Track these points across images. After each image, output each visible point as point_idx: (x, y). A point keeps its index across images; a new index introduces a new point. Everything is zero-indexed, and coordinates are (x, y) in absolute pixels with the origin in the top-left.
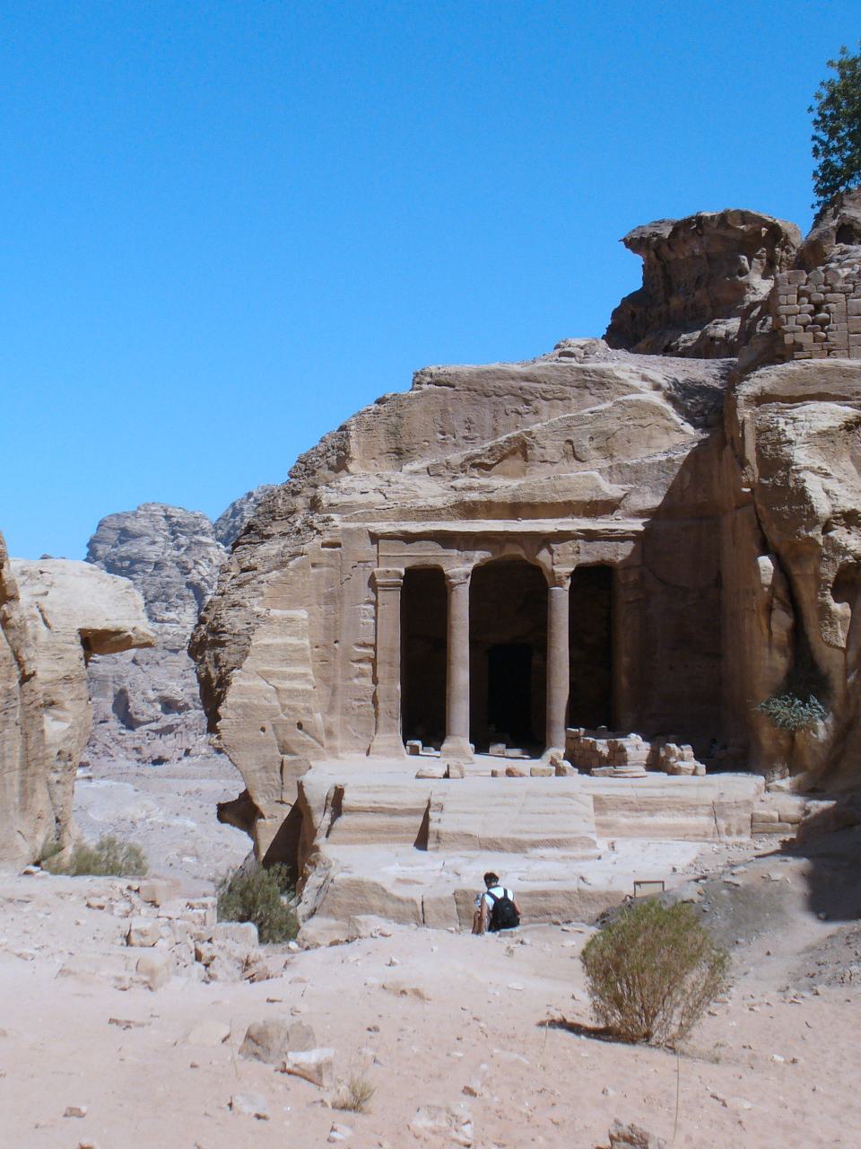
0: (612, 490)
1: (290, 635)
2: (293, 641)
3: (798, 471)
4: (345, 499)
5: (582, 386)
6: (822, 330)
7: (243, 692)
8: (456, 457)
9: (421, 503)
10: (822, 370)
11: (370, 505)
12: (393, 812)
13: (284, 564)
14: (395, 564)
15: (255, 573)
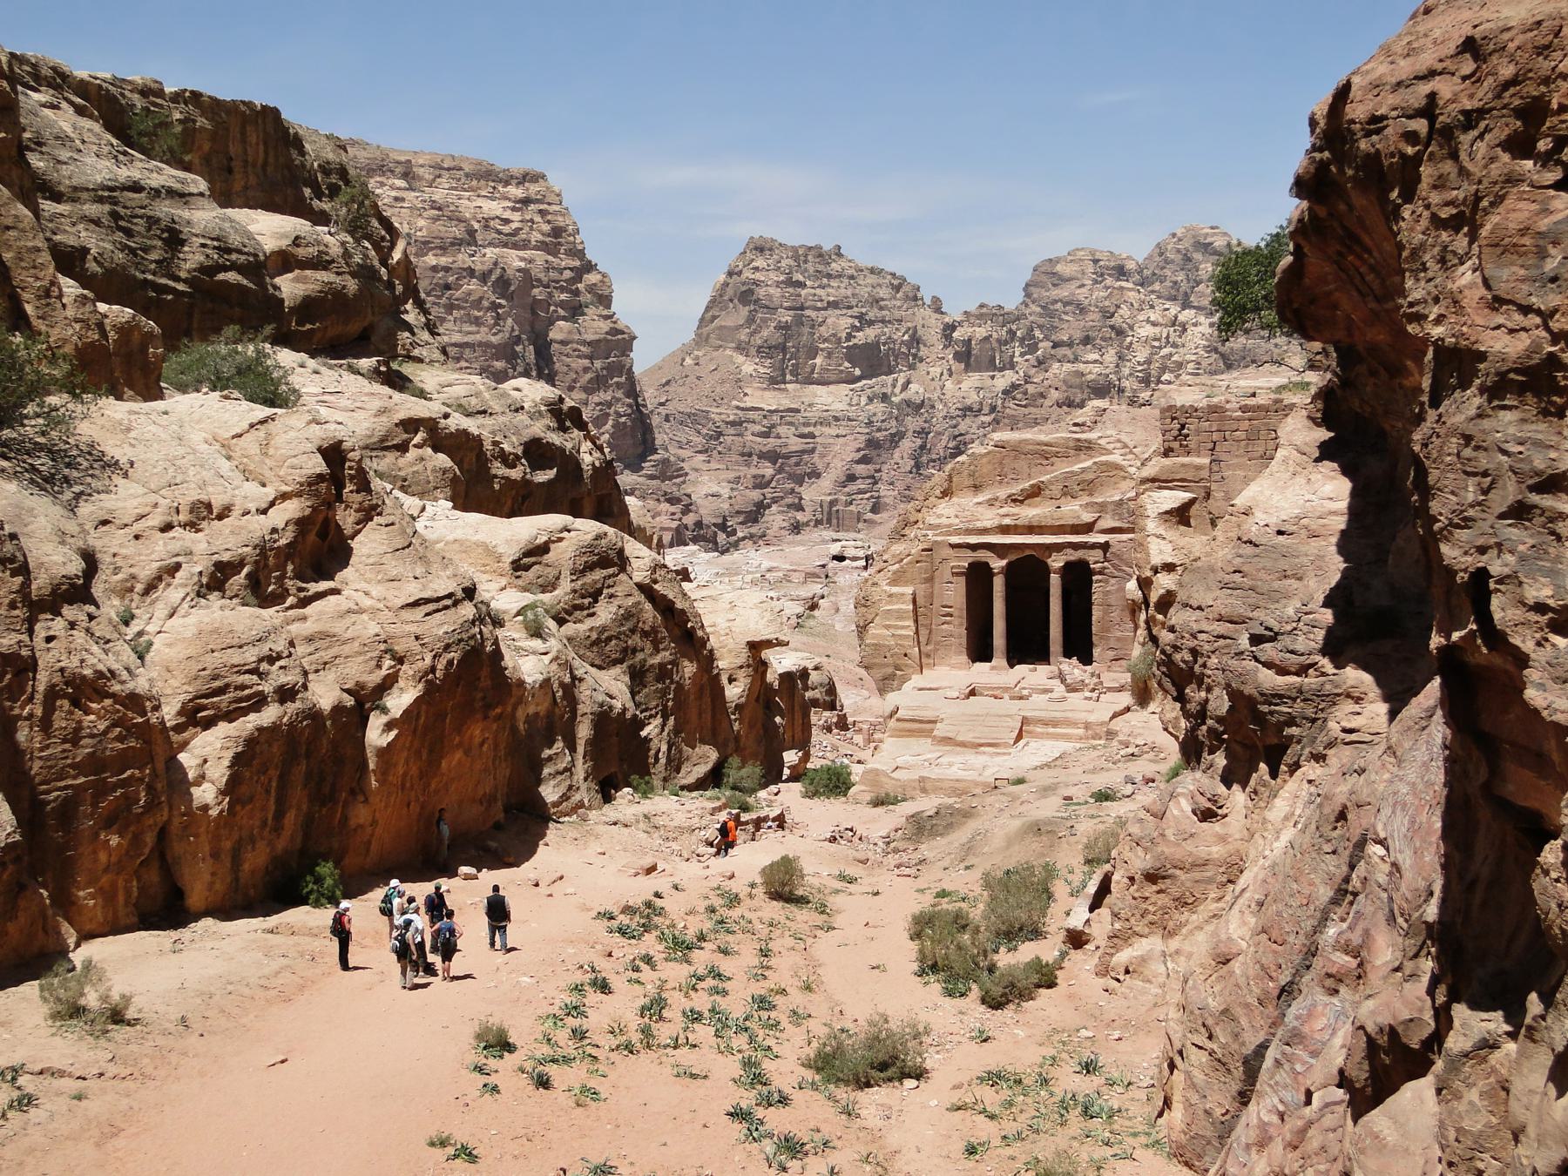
0: (1087, 517)
2: (903, 607)
4: (938, 521)
5: (1078, 449)
7: (875, 636)
8: (1002, 493)
10: (1183, 465)
11: (950, 526)
12: (921, 722)
14: (964, 561)
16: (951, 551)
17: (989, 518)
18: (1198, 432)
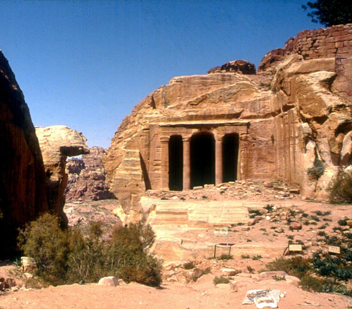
0: (237, 110)
1: (134, 157)
2: (135, 159)
3: (317, 93)
6: (316, 49)
9: (175, 116)
10: (317, 62)
11: (158, 117)
13: (132, 135)
15: (123, 139)
16: (160, 129)
17: (179, 114)
18: (325, 44)
